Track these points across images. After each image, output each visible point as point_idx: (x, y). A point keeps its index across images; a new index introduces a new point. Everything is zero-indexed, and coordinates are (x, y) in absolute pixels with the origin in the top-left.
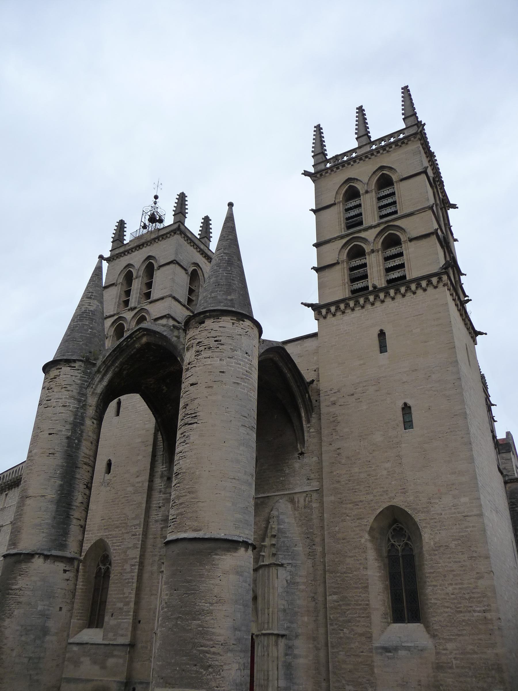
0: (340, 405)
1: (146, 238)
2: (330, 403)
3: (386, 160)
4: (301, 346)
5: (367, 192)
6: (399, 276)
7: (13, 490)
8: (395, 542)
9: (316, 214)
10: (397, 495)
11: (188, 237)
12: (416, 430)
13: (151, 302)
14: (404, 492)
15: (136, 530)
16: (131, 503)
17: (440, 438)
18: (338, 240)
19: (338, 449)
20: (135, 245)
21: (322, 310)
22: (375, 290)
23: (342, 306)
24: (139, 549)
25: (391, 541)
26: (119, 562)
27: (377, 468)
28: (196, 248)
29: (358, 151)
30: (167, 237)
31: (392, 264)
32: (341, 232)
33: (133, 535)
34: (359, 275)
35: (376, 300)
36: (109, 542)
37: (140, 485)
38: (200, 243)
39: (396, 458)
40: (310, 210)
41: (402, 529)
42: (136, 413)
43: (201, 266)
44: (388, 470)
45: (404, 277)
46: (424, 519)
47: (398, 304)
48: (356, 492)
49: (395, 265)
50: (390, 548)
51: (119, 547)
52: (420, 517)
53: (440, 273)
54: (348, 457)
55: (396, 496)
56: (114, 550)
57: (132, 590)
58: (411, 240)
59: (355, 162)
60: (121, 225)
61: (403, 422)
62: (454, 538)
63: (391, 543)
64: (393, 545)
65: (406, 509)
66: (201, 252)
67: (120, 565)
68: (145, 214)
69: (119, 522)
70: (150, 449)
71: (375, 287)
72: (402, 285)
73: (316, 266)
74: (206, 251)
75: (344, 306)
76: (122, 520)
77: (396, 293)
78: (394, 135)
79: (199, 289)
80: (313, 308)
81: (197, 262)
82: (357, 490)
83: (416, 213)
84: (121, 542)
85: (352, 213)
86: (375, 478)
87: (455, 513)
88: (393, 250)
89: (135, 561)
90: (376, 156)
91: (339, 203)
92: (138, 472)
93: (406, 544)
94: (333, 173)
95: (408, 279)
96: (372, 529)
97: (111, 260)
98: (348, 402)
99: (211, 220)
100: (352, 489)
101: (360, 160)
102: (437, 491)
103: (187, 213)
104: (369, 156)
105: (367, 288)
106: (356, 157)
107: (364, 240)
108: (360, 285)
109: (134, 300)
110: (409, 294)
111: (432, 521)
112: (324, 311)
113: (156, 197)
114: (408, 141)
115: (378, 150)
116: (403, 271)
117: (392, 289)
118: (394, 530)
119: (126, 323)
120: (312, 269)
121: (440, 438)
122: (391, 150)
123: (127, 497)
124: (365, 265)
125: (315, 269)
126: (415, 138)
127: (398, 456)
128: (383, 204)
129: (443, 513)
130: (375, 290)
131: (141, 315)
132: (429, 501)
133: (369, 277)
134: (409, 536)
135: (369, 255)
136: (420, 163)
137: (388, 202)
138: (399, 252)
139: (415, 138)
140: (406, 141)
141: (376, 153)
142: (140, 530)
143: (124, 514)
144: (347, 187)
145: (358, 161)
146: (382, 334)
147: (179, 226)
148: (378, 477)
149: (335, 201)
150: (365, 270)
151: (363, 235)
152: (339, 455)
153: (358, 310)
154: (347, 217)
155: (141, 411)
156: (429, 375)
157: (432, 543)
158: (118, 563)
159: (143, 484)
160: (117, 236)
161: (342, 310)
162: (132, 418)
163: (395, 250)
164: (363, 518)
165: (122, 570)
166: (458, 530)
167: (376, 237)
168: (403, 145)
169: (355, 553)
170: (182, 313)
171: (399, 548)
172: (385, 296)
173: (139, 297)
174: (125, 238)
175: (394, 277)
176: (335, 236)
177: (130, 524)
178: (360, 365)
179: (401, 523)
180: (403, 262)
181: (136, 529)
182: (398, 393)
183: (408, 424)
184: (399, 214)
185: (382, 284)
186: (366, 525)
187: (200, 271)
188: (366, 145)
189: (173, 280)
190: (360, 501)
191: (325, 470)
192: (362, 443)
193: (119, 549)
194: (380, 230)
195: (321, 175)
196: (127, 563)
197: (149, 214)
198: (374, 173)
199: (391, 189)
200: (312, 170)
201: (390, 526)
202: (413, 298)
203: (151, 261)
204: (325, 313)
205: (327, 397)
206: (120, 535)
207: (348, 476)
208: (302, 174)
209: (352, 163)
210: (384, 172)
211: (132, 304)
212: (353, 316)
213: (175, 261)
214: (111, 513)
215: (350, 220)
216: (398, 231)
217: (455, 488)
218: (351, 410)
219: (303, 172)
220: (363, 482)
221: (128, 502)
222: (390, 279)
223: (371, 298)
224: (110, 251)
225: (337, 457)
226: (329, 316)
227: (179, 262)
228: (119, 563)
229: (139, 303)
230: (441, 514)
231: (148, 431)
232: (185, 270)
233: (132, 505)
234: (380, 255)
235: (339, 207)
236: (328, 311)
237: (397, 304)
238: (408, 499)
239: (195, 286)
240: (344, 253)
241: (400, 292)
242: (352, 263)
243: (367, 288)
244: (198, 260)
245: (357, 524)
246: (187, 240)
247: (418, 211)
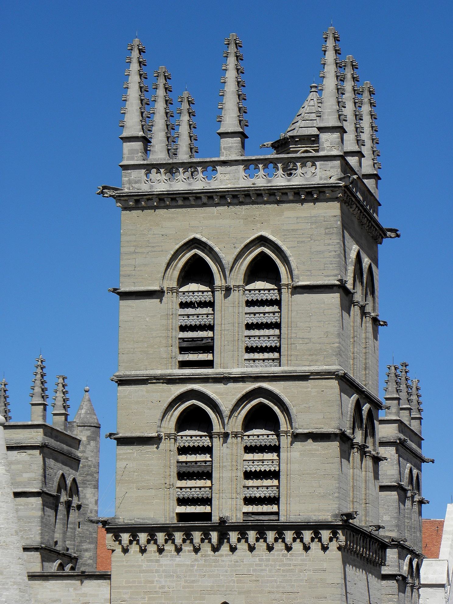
4: (75, 589)
34: (196, 470)
47: (259, 561)
71: (223, 521)
72: (271, 528)
115: (259, 192)
136: (334, 258)
137: (264, 321)
153: (189, 551)
194: (244, 392)
198: (248, 247)
202: (286, 556)
204: (128, 542)
242: (184, 438)
247: (318, 373)
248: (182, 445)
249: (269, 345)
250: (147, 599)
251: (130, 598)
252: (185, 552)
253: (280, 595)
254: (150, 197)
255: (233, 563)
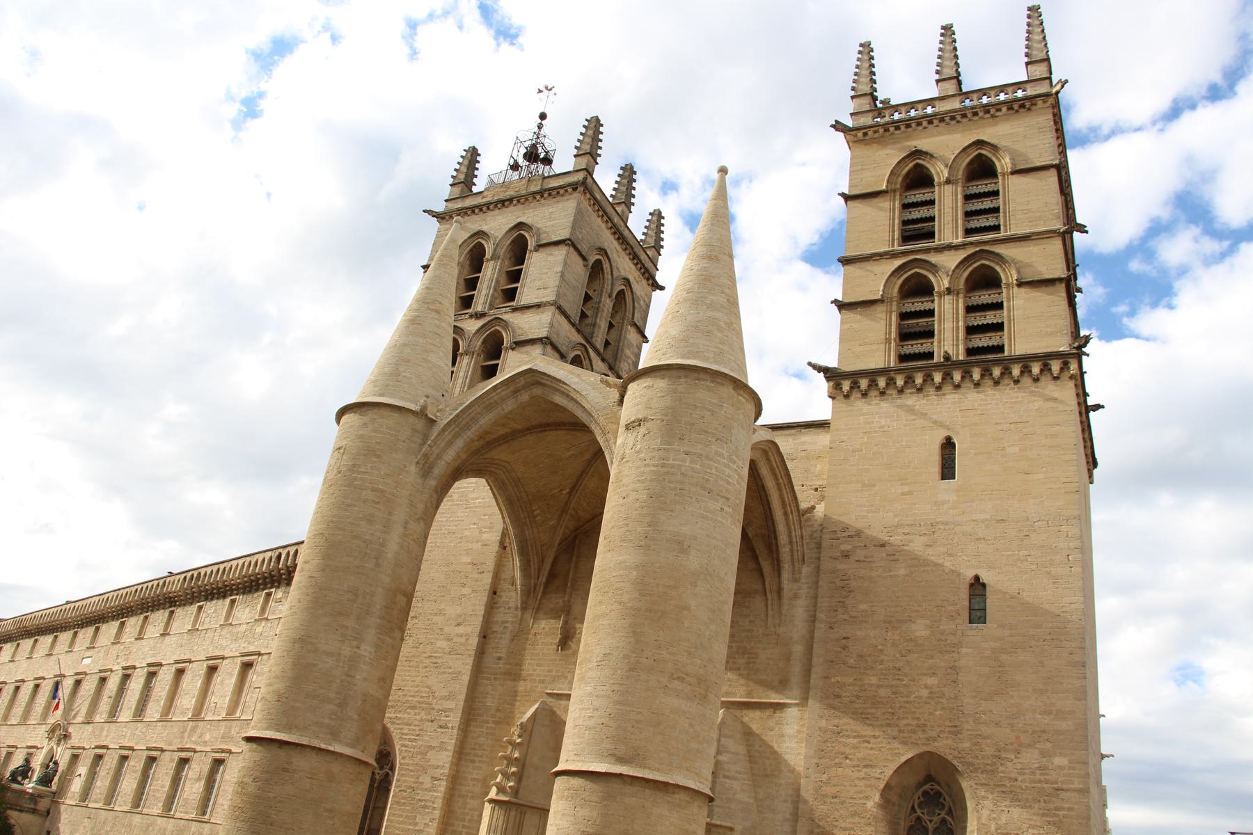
0: (857, 561)
1: (518, 189)
2: (839, 554)
3: (989, 133)
5: (948, 182)
6: (990, 344)
7: (214, 602)
8: (923, 813)
9: (849, 203)
10: (941, 736)
11: (595, 199)
12: (991, 628)
13: (515, 310)
14: (955, 731)
15: (448, 719)
16: (443, 670)
17: (1031, 647)
18: (886, 259)
19: (844, 638)
20: (496, 198)
21: (842, 382)
22: (946, 363)
23: (882, 382)
24: (451, 754)
25: (916, 812)
26: (411, 768)
27: (912, 683)
28: (607, 222)
29: (937, 103)
30: (558, 193)
31: (980, 319)
32: (893, 246)
33: (441, 727)
34: (917, 330)
35: (944, 381)
36: (396, 731)
37: (462, 640)
38: (614, 212)
39: (949, 670)
40: (839, 194)
41: (939, 794)
42: (466, 508)
43: (609, 253)
44: (932, 690)
45: (1000, 349)
46: (984, 784)
48: (867, 718)
49: (985, 323)
50: (913, 823)
51: (414, 744)
52: (976, 778)
53: (1066, 354)
54: (861, 656)
55: (939, 736)
56: (403, 745)
57: (430, 821)
58: (1020, 284)
59: (930, 122)
60: (472, 157)
61: (968, 609)
62: (1033, 823)
63: (916, 814)
64: (919, 818)
65: (955, 762)
66: (613, 230)
67: (412, 773)
68: (519, 144)
69: (417, 699)
70: (487, 579)
71: (947, 358)
72: (997, 362)
73: (840, 299)
74: (622, 228)
75: (885, 382)
76: (422, 697)
77: (982, 376)
78: (1006, 88)
79: (601, 297)
80: (828, 375)
81: (606, 248)
82: (869, 716)
83: (1033, 238)
84: (418, 735)
85: (916, 214)
86: (905, 699)
87: (1040, 781)
88: (984, 295)
89: (442, 771)
90: (970, 120)
91: (895, 191)
92: (460, 616)
93: (944, 821)
94: (887, 134)
95: (1006, 353)
96: (887, 786)
97: (447, 217)
98: (872, 556)
99: (635, 173)
100: (862, 713)
101: (940, 121)
102: (1014, 738)
103: (600, 155)
104: (958, 118)
105: (930, 355)
106: (934, 115)
107: (934, 268)
108: (917, 347)
109: (481, 300)
110: (1006, 381)
111: (998, 790)
112: (846, 385)
113: (543, 116)
114: (1032, 105)
116: (998, 338)
117: (977, 366)
118: (925, 793)
119: (462, 340)
120: (832, 302)
121: (1031, 647)
122: (998, 114)
123: (435, 657)
124: (930, 313)
125: (838, 304)
126: (1045, 102)
127: (952, 668)
128: (974, 208)
129: (1020, 779)
130: (946, 363)
131: (493, 329)
132: (998, 754)
133: (936, 337)
134: (950, 809)
135: (940, 296)
137: (983, 207)
138: (995, 302)
139: (1045, 102)
140: (1027, 104)
141: (972, 114)
142: (455, 719)
143: (427, 687)
144: (911, 165)
145: (936, 122)
146: (948, 446)
147: (585, 179)
148: (912, 698)
149: (887, 186)
150: (930, 323)
151: (933, 258)
152: (844, 649)
154: (906, 219)
155: (476, 507)
156: (1027, 533)
157: (993, 827)
158: (408, 769)
159: (467, 639)
160: (462, 177)
161: (880, 389)
162: (458, 517)
163: (987, 296)
164: (875, 766)
165: (416, 782)
166: (1041, 812)
167: (957, 267)
168: (1022, 110)
169: (853, 823)
170: (568, 338)
171: (931, 826)
172: (963, 378)
173: (493, 295)
174: (475, 180)
175: (981, 345)
176: (882, 250)
177: (437, 707)
178: (903, 494)
179: (938, 784)
180: (1000, 321)
181: (448, 716)
182: (966, 556)
183: (977, 614)
184: (1002, 234)
185: (958, 355)
186: (879, 779)
187: (608, 265)
188: (953, 96)
189: (562, 276)
190: (874, 736)
191: (817, 672)
192: (889, 634)
193: (414, 747)
195: (865, 134)
196: (426, 773)
197: (527, 144)
199: (991, 183)
200: (849, 122)
201: (920, 785)
202: (1014, 389)
203: (522, 232)
204: (848, 388)
205: (834, 542)
206: (416, 723)
207: (857, 688)
208: (832, 126)
209: (925, 124)
210: (983, 152)
211: (479, 305)
212: (899, 401)
213: (569, 242)
214: (403, 680)
215: (911, 227)
216: (998, 264)
217: (1047, 740)
218: (876, 573)
219: (834, 123)
220: (882, 703)
221: (437, 667)
222: (973, 348)
223: (938, 378)
224: (446, 201)
225: (840, 652)
226: (856, 394)
227: (576, 243)
228: (411, 771)
229: (491, 307)
230: (1016, 780)
231: (485, 545)
232: (584, 259)
233: (445, 673)
234: (961, 301)
235: (892, 198)
236: (855, 385)
237: (982, 396)
238: (960, 745)
239: (595, 291)
240: (895, 284)
241: (991, 374)
243: (930, 355)
244: (606, 244)
245: (862, 774)
246: (594, 204)
248: (904, 311)
249: (987, 224)
250: (865, 439)
251: (849, 438)
252: (906, 394)
253: (1007, 425)
254: (877, 128)
255: (956, 400)
